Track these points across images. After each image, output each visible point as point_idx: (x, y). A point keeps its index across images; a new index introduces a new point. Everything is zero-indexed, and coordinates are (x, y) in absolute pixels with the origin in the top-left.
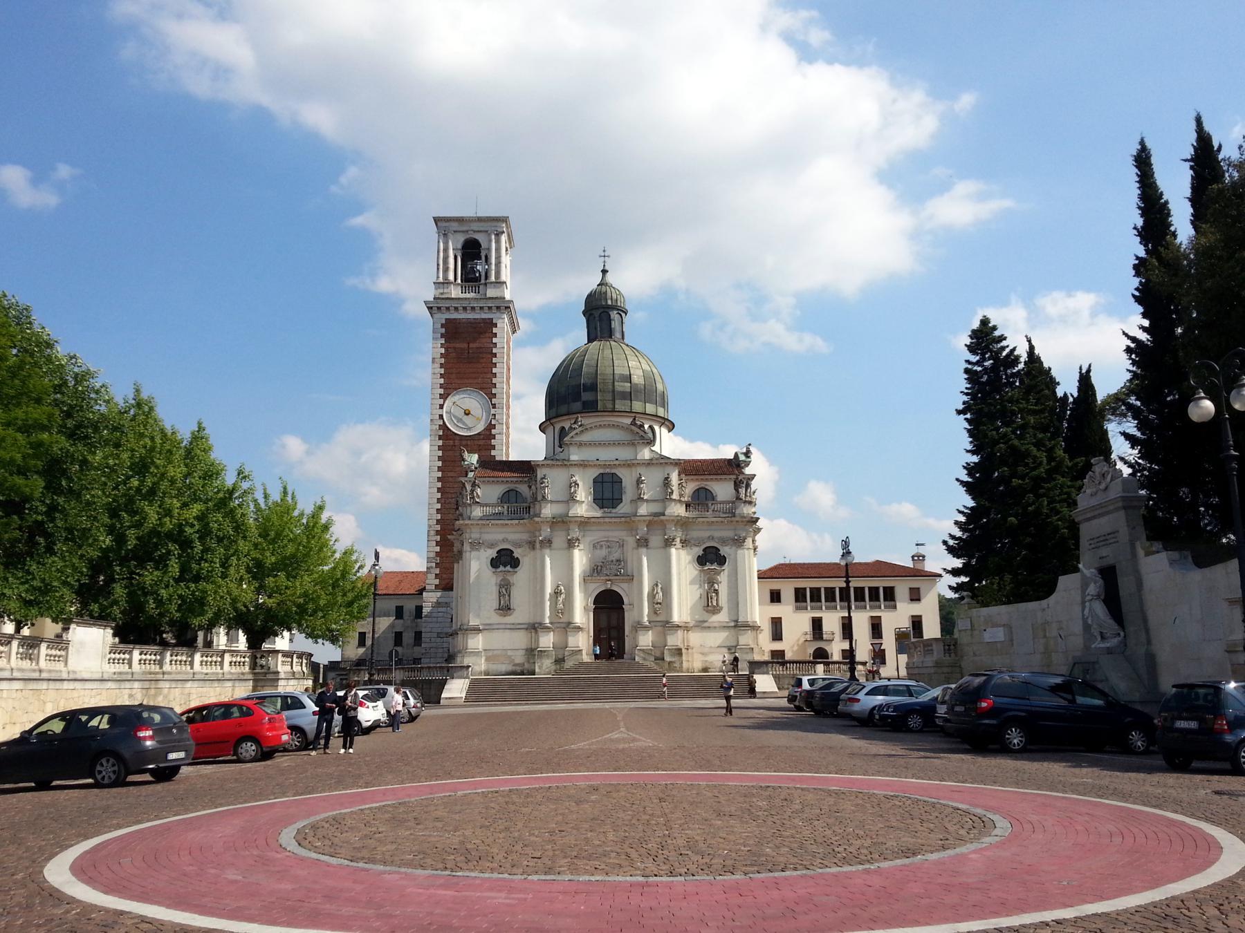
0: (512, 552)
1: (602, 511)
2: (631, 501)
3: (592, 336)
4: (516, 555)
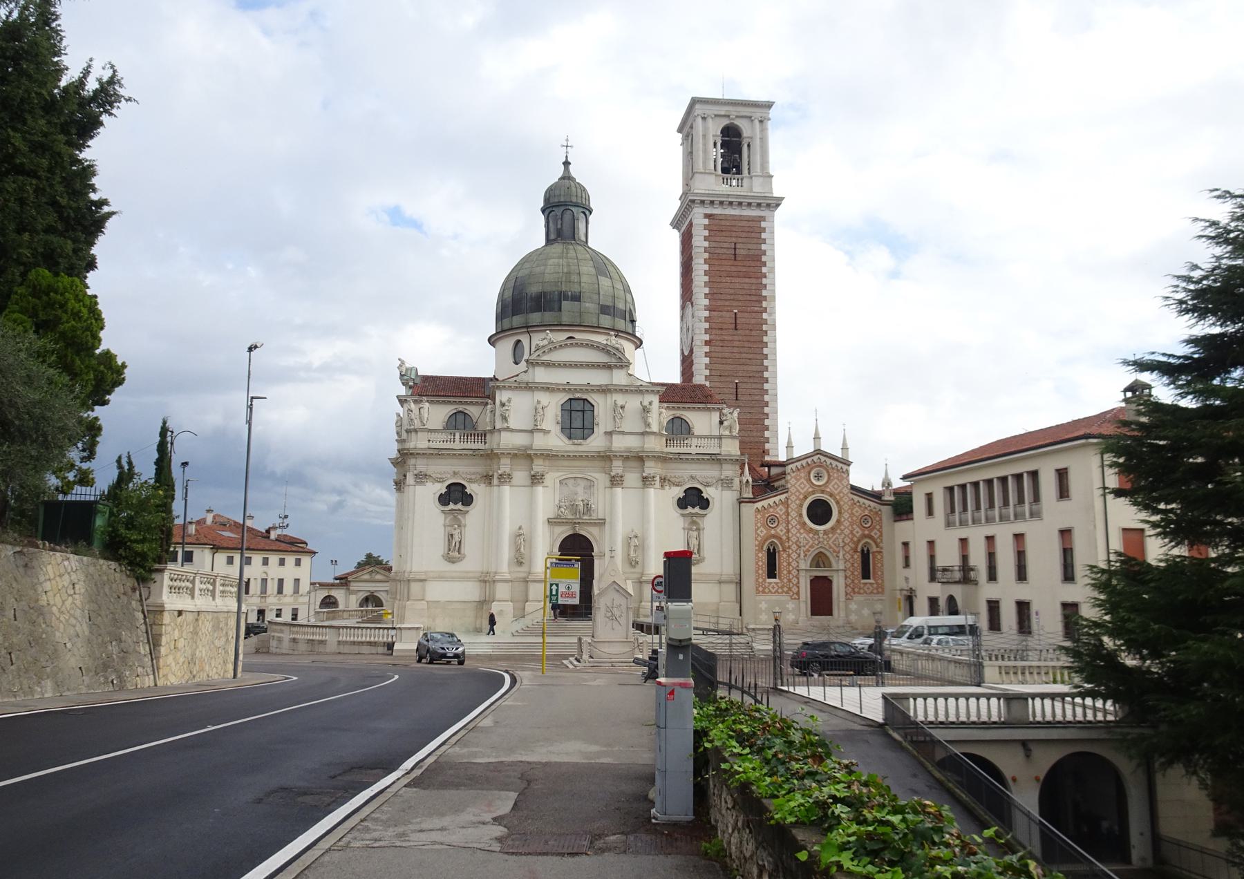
0: (464, 487)
1: (571, 442)
2: (606, 433)
3: (552, 237)
4: (468, 491)
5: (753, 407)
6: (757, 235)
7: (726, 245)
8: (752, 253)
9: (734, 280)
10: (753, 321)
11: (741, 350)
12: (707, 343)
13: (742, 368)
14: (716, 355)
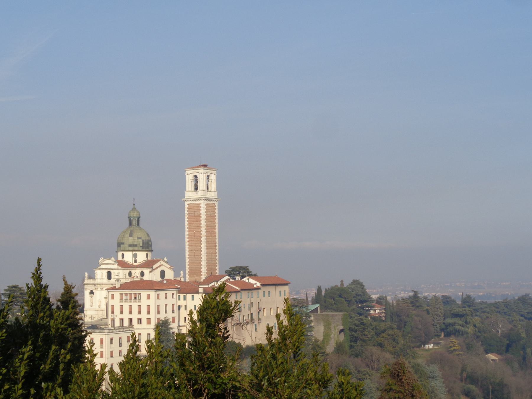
5: (198, 259)
6: (199, 209)
7: (192, 213)
8: (198, 214)
9: (195, 222)
10: (198, 234)
11: (196, 243)
12: (188, 241)
13: (196, 248)
14: (191, 245)
